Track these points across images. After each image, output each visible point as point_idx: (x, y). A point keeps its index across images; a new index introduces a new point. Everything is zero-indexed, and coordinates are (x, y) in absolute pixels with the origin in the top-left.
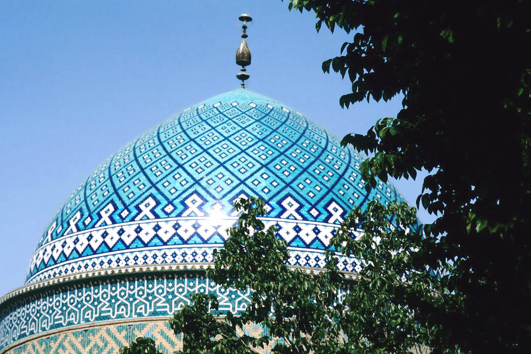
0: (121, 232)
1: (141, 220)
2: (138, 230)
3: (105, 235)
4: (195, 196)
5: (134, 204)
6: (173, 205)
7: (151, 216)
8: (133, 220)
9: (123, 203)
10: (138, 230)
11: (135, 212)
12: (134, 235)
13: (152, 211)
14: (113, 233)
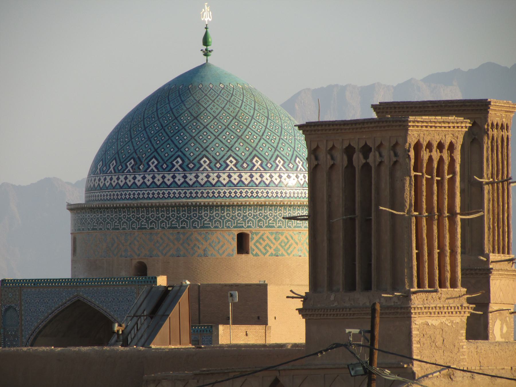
0: (163, 177)
1: (175, 171)
2: (174, 177)
3: (154, 178)
4: (205, 159)
5: (170, 161)
6: (193, 163)
7: (180, 169)
8: (170, 171)
9: (163, 160)
10: (174, 177)
11: (170, 166)
12: (151, 180)
13: (180, 166)
14: (159, 177)
